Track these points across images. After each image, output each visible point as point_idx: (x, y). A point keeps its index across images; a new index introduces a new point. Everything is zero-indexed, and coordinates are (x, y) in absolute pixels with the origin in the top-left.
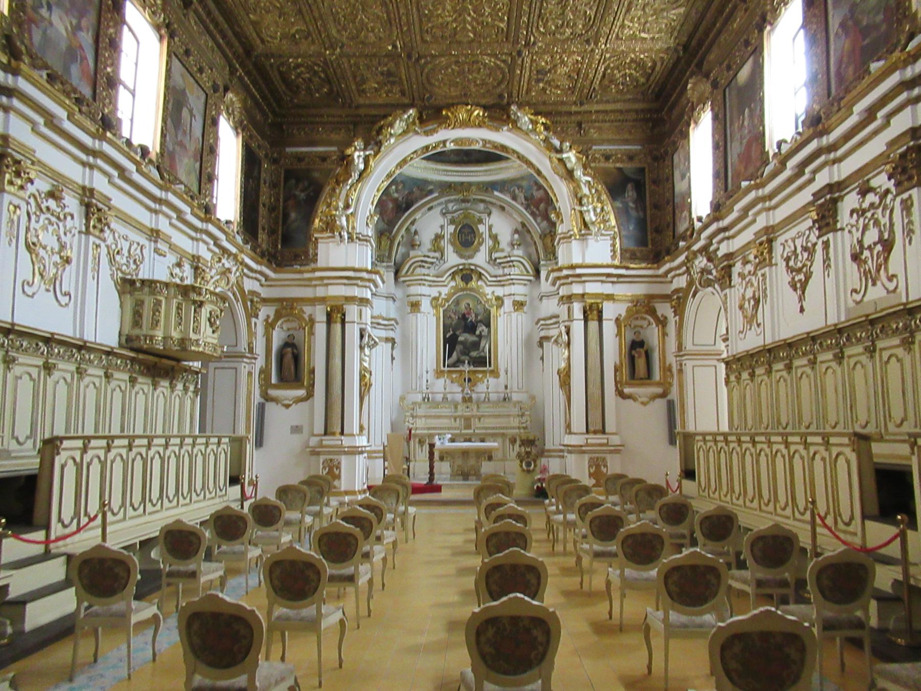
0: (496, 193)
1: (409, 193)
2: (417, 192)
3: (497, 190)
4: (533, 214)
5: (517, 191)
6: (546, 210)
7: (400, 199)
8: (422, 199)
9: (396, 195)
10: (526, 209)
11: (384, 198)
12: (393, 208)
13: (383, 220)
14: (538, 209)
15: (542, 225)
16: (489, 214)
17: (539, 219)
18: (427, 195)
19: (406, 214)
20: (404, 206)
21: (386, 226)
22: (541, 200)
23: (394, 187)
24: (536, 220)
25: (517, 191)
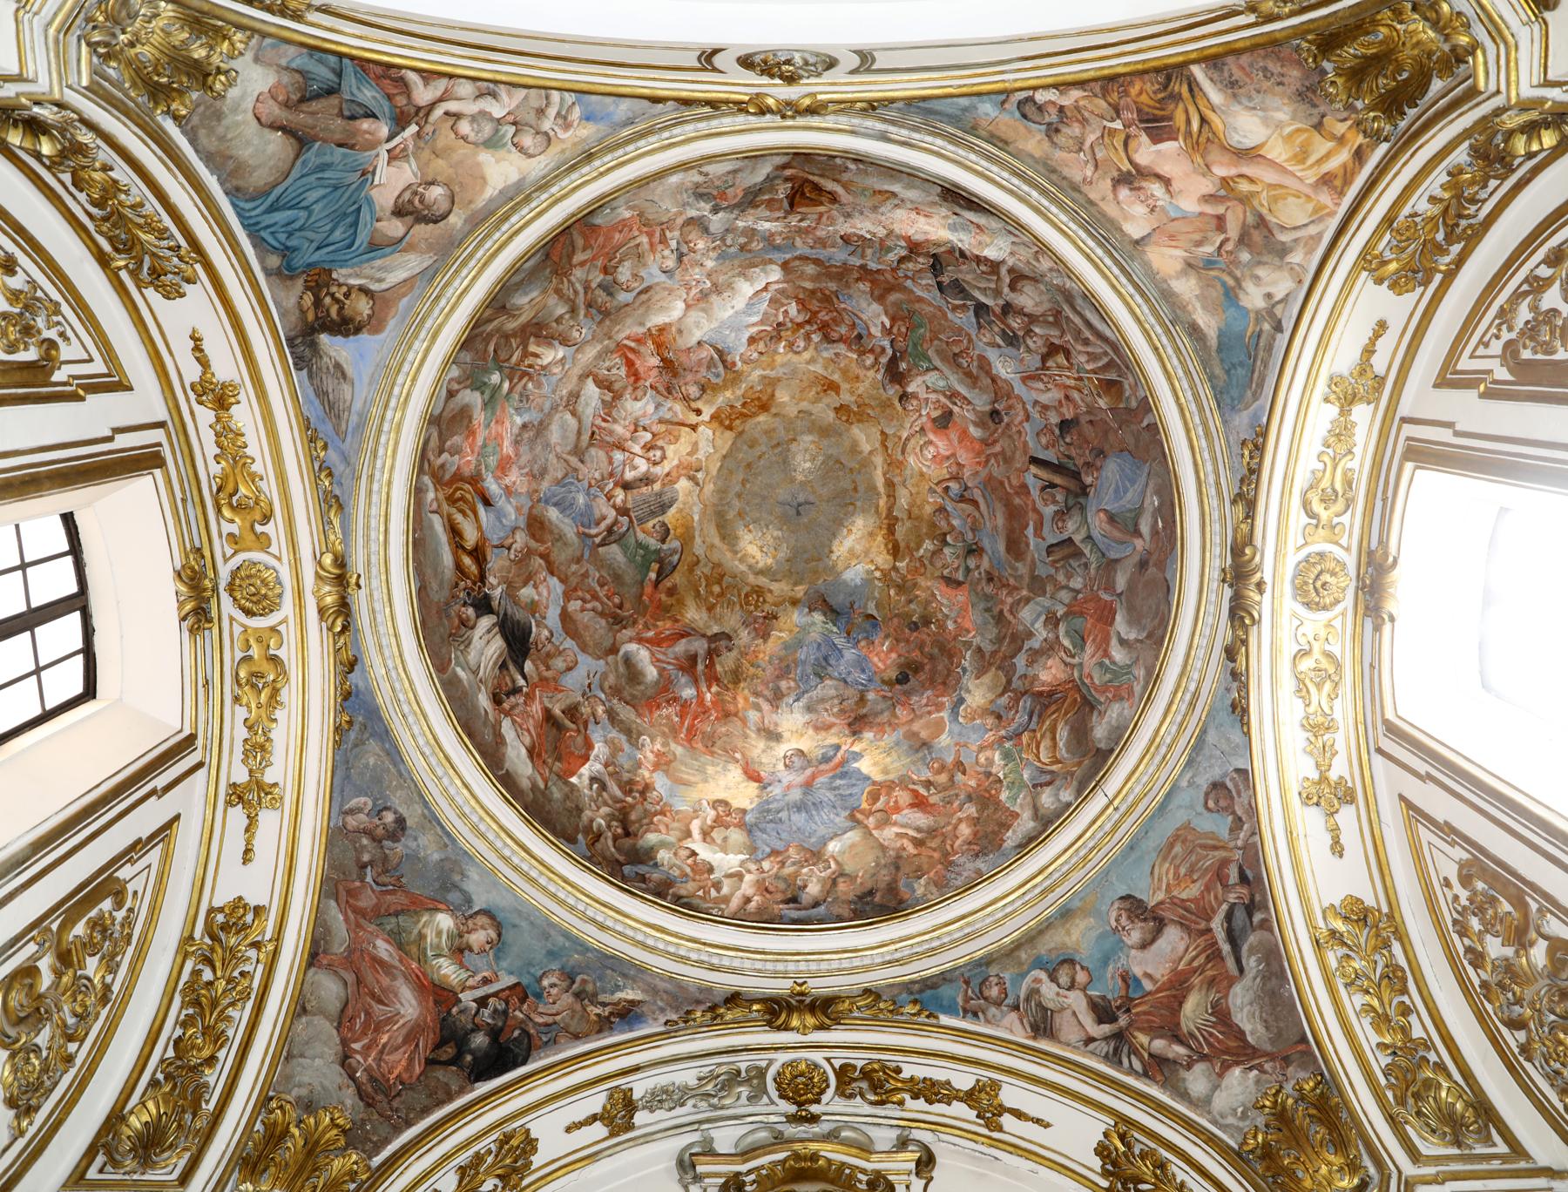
0: (945, 1020)
1: (519, 992)
2: (558, 1004)
3: (951, 1010)
4: (1158, 1068)
5: (1048, 990)
6: (1222, 1015)
7: (467, 998)
8: (577, 1037)
9: (447, 970)
10: (1114, 1058)
11: (383, 949)
12: (412, 1036)
13: (345, 1059)
14: (1177, 1038)
15: (1220, 1101)
16: (926, 1163)
17: (1197, 1080)
18: (604, 1025)
19: (484, 1088)
20: (480, 1040)
21: (349, 1097)
22: (1178, 986)
23: (445, 921)
24: (1184, 1095)
25: (1048, 990)
